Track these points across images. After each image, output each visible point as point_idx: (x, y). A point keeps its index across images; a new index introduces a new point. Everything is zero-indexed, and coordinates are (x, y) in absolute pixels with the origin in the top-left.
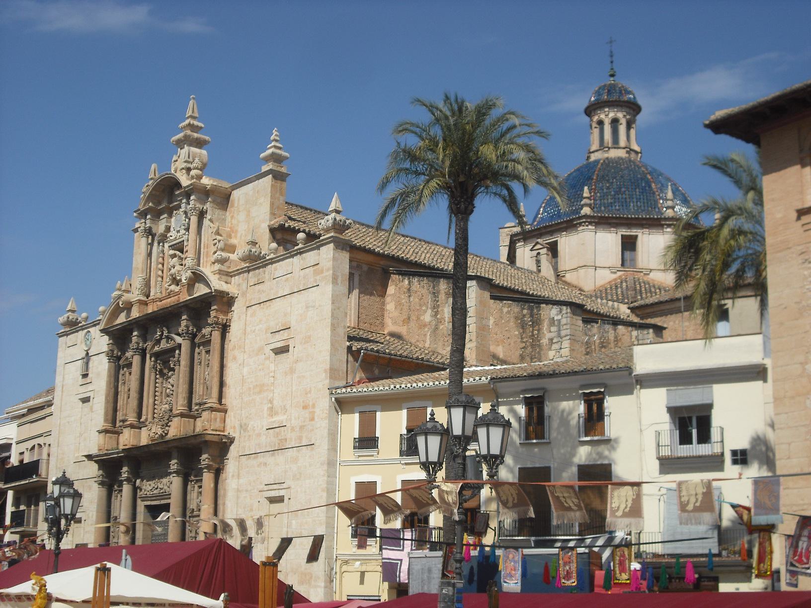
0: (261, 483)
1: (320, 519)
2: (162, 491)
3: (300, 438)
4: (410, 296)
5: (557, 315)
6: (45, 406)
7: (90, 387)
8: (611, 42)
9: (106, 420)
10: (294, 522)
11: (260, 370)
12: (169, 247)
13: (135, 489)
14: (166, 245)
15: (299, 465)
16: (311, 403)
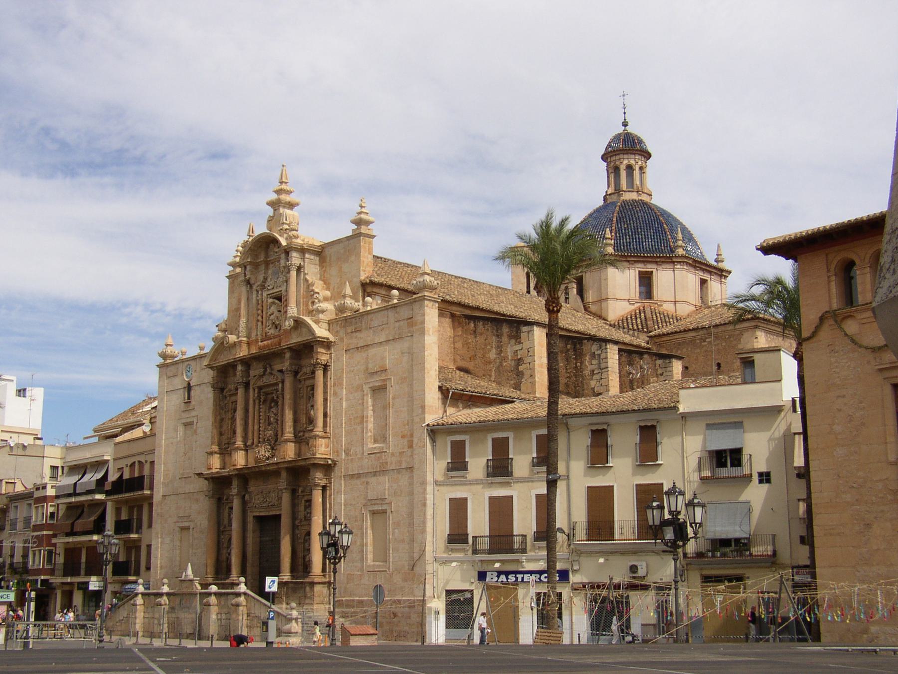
3: (400, 462)
4: (476, 337)
5: (597, 350)
6: (135, 425)
7: (193, 413)
8: (624, 95)
12: (267, 295)
13: (244, 503)
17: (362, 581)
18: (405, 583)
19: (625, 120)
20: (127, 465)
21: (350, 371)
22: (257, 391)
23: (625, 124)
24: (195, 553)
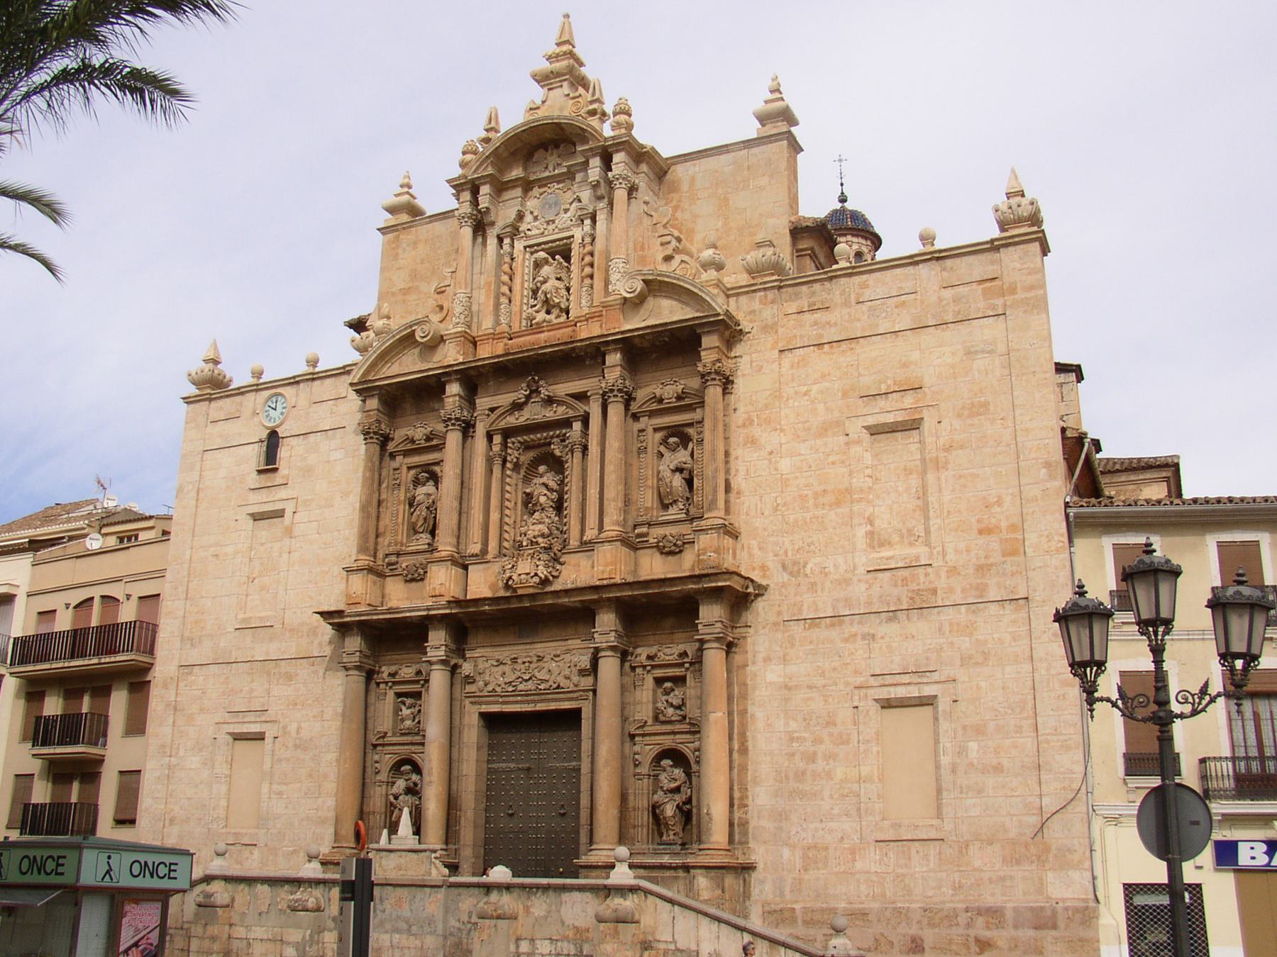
0: (857, 672)
1: (1062, 738)
2: (542, 687)
3: (982, 589)
6: (63, 538)
7: (283, 493)
8: (840, 160)
10: (973, 745)
11: (833, 463)
12: (525, 247)
14: (519, 245)
15: (979, 637)
16: (1004, 524)
17: (859, 865)
18: (1015, 868)
19: (842, 193)
20: (67, 606)
21: (796, 393)
22: (497, 439)
23: (843, 200)
24: (280, 793)
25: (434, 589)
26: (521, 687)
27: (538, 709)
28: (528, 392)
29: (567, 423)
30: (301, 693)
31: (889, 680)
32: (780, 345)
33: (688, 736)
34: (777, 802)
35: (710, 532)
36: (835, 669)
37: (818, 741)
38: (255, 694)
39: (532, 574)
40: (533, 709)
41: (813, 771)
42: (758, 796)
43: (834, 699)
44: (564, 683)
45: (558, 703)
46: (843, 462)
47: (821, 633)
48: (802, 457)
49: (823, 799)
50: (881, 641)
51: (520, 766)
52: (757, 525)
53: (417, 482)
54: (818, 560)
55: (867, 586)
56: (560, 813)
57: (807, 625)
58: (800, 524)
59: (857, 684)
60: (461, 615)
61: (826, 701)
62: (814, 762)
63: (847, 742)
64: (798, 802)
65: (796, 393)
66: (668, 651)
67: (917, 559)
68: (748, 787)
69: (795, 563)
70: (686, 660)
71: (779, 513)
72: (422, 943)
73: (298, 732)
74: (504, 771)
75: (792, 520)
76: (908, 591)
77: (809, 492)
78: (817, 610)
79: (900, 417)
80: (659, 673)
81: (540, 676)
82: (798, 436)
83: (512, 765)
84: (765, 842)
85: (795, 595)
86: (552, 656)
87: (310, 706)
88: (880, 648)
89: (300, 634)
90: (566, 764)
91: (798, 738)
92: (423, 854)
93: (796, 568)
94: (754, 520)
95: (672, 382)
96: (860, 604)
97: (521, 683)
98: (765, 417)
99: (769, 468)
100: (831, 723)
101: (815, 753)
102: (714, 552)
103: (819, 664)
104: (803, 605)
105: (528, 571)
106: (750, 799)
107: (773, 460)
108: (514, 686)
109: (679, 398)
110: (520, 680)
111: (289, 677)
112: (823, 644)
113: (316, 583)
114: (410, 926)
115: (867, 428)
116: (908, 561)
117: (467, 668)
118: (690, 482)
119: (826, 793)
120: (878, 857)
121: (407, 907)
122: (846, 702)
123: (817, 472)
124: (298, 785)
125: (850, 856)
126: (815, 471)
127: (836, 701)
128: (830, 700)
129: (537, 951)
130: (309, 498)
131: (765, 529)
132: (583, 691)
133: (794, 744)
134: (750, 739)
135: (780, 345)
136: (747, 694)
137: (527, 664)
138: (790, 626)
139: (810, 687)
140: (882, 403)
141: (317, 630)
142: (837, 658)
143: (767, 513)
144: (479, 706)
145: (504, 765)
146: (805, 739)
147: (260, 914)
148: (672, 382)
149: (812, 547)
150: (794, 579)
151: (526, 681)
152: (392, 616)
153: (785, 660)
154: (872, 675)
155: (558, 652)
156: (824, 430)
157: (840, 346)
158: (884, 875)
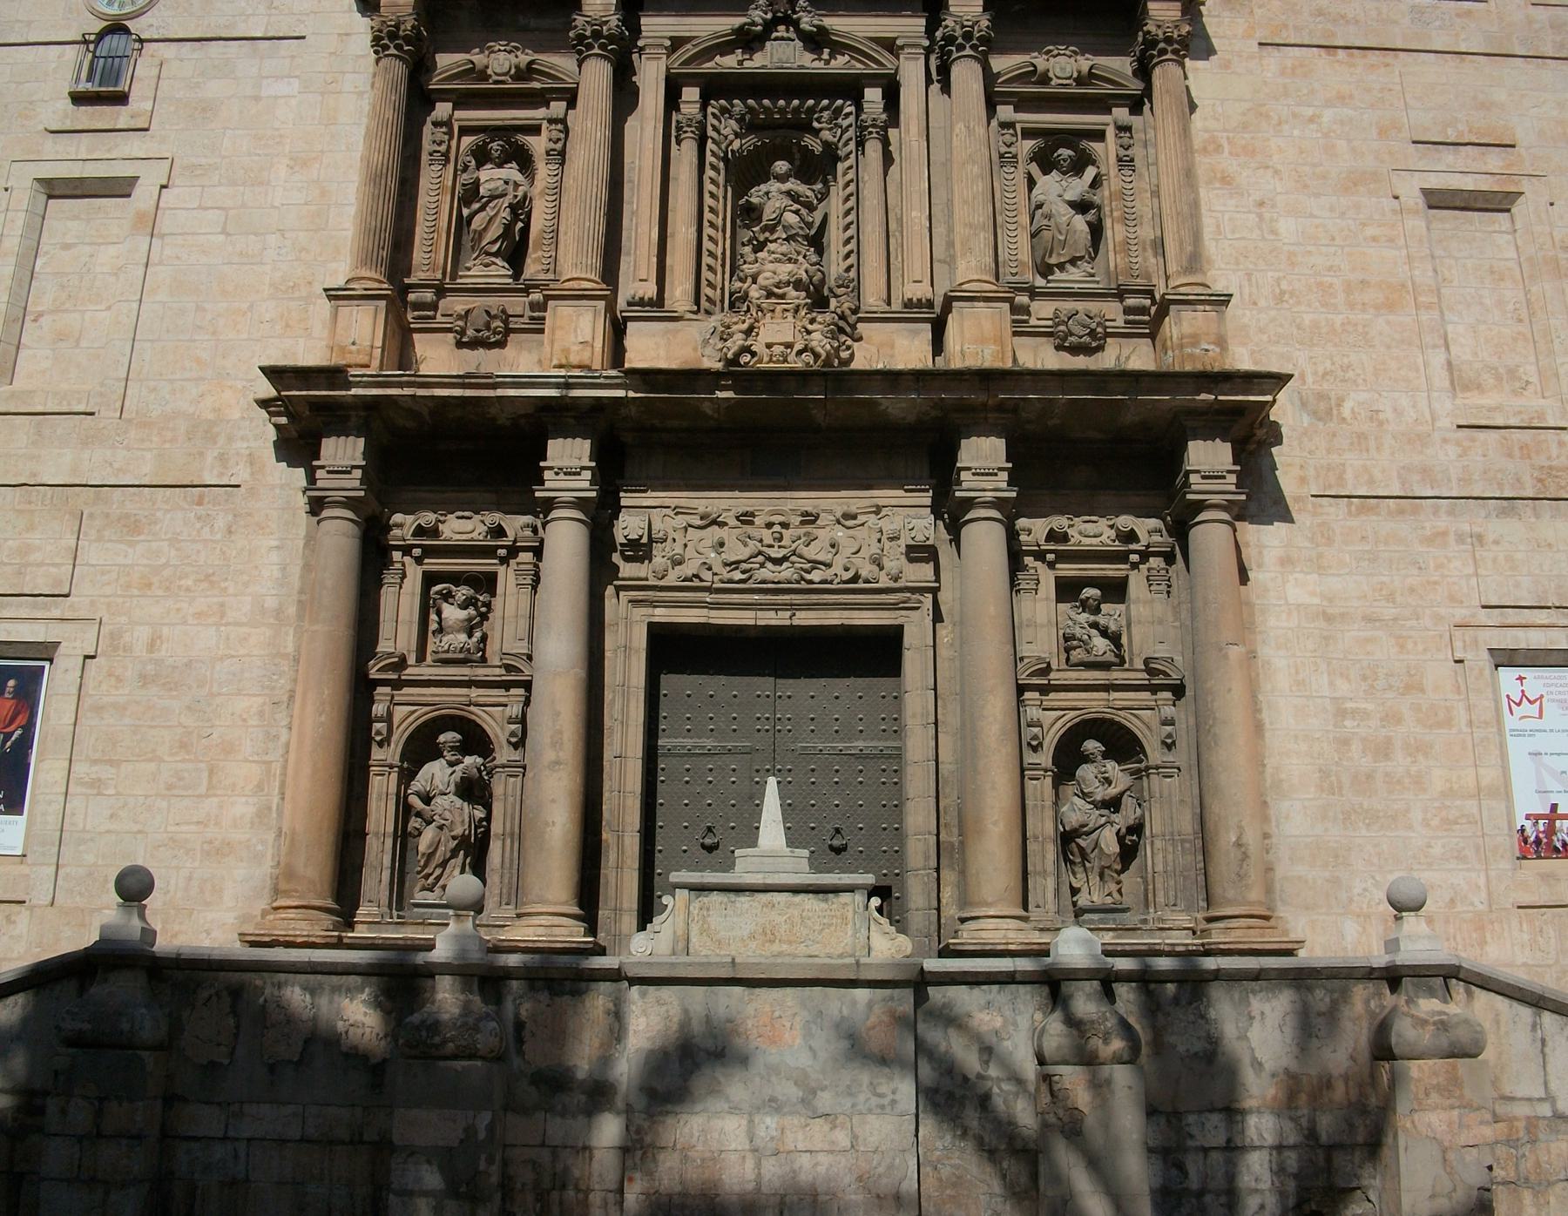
0: (1453, 599)
7: (135, 146)
9: (365, 259)
11: (1374, 239)
22: (691, 94)
24: (97, 785)
25: (566, 351)
26: (765, 573)
27: (796, 622)
28: (769, 16)
29: (851, 88)
30: (163, 560)
31: (1513, 616)
32: (1257, 35)
33: (1146, 695)
34: (1326, 830)
35: (1201, 307)
36: (1412, 590)
37: (1392, 718)
38: (36, 557)
39: (798, 347)
40: (788, 623)
41: (1387, 774)
42: (1287, 817)
43: (1415, 643)
44: (867, 570)
45: (846, 614)
46: (1391, 240)
47: (1380, 522)
48: (1317, 221)
49: (1410, 828)
50: (1494, 548)
51: (730, 745)
52: (1246, 320)
53: (482, 156)
54: (1363, 396)
55: (1459, 450)
56: (832, 848)
57: (1353, 508)
58: (1324, 330)
59: (1458, 620)
60: (633, 410)
61: (1402, 647)
62: (1387, 757)
63: (1448, 722)
64: (1364, 832)
65: (1295, 115)
66: (1090, 528)
67: (1541, 416)
68: (1268, 799)
69: (1321, 396)
70: (1134, 547)
71: (1285, 305)
72: (855, 1137)
73: (152, 646)
74: (690, 755)
75: (1307, 322)
76: (1532, 466)
77: (1335, 280)
78: (1371, 482)
79: (1485, 184)
80: (1069, 570)
81: (811, 552)
82: (1306, 186)
83: (709, 743)
84: (1307, 908)
85: (1329, 451)
86: (839, 515)
87: (188, 589)
88: (1495, 560)
89: (169, 435)
90: (841, 745)
91: (1354, 712)
92: (845, 898)
93: (1322, 406)
94: (1239, 312)
95: (1067, 52)
96: (1449, 480)
97: (762, 565)
98: (1243, 142)
99: (1260, 229)
100: (1413, 686)
101: (1389, 741)
102: (1214, 343)
103: (1384, 579)
104: (1344, 471)
105: (790, 339)
106: (1274, 824)
107: (1267, 216)
108: (743, 572)
109: (1080, 81)
110: (760, 559)
111: (132, 527)
112: (1386, 543)
113: (214, 333)
114: (814, 1092)
115: (1427, 193)
116: (1525, 417)
117: (628, 526)
118: (1096, 230)
119: (1417, 815)
120: (1526, 937)
121: (798, 1041)
122: (1439, 650)
123: (1347, 250)
124: (152, 766)
125: (1474, 935)
126: (1342, 247)
127: (1420, 647)
128: (1410, 646)
129: (1190, 1143)
130: (203, 161)
131: (1261, 331)
132: (913, 590)
133: (1347, 723)
134: (1264, 706)
135: (1257, 35)
136: (1253, 623)
137: (777, 528)
138: (1321, 506)
139: (1368, 619)
140: (1448, 157)
141: (216, 429)
142: (1416, 572)
143: (1262, 303)
144: (650, 611)
145: (688, 742)
146: (1365, 715)
147: (272, 1069)
148: (1067, 52)
149: (1350, 374)
150: (1321, 425)
151: (778, 562)
152: (469, 393)
153: (1320, 567)
154: (1484, 607)
155: (853, 510)
156: (1354, 182)
157: (1365, 56)
158: (1539, 970)
